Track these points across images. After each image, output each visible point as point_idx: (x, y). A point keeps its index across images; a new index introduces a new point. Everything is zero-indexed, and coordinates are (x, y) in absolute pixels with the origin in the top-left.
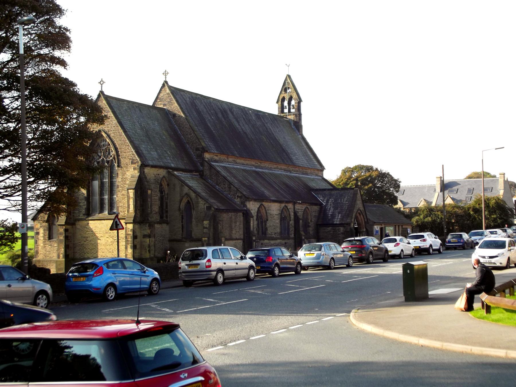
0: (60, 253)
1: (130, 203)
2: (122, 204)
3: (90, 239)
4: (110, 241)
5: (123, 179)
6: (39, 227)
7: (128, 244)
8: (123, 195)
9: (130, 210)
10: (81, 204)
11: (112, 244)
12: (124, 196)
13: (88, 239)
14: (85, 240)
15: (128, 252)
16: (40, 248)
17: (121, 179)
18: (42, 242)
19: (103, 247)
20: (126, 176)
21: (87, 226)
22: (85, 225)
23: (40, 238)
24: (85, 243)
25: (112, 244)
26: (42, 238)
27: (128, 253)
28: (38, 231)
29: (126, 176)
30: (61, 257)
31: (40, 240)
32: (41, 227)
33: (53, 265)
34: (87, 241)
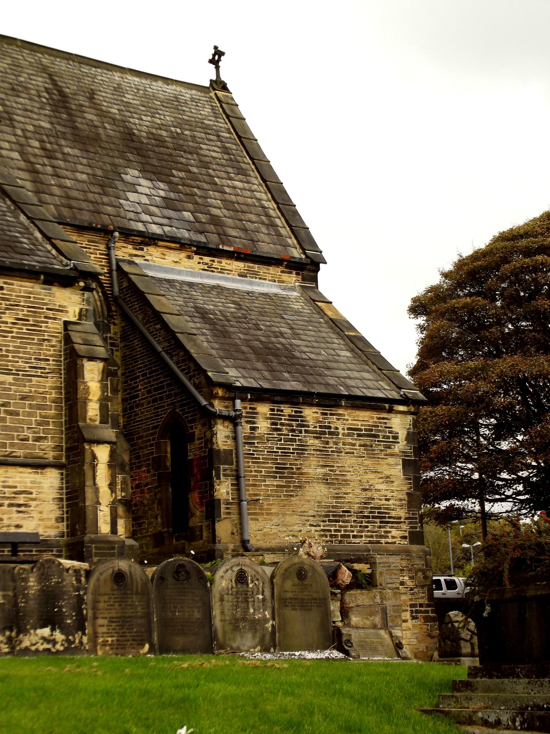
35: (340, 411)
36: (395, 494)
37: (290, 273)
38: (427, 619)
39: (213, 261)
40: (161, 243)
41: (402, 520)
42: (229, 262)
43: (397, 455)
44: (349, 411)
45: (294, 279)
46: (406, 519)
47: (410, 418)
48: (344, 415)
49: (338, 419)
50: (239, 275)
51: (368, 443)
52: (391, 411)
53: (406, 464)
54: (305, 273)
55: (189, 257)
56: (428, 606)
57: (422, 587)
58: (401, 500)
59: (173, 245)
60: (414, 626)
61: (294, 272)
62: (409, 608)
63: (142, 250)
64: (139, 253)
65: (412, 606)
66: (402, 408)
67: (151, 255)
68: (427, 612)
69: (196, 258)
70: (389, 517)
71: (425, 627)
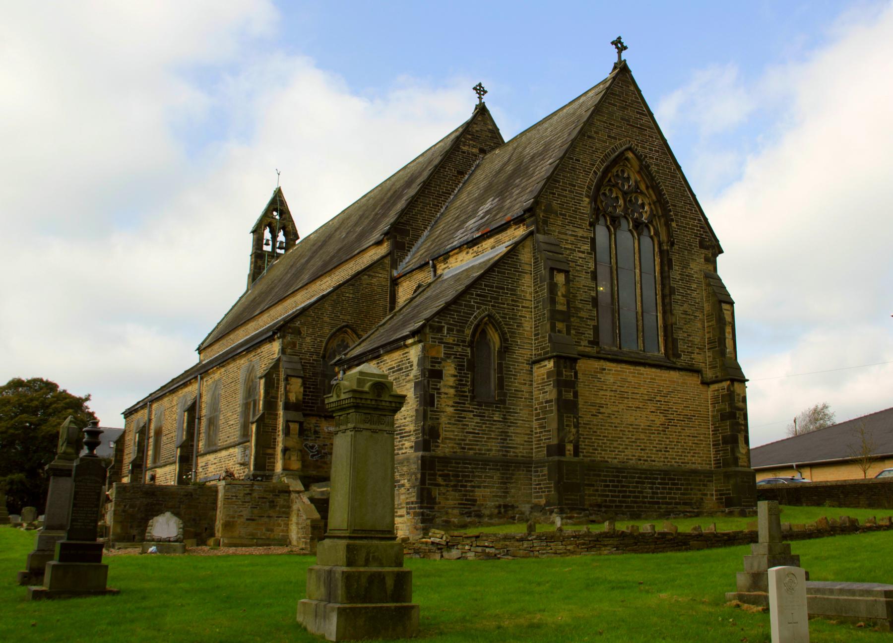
0: (566, 440)
1: (727, 334)
2: (685, 335)
3: (609, 411)
4: (658, 422)
5: (683, 275)
6: (442, 355)
7: (740, 433)
8: (685, 313)
9: (728, 350)
10: (583, 314)
11: (663, 431)
12: (689, 317)
13: (602, 410)
14: (594, 412)
15: (740, 452)
16: (444, 419)
17: (680, 274)
18: (451, 403)
19: (642, 436)
20: (689, 271)
21: (599, 375)
22: (595, 372)
23: (443, 390)
24: (595, 421)
25: (665, 431)
26: (452, 391)
27: (739, 455)
28: (437, 367)
29: (689, 271)
30: (567, 452)
31: (442, 396)
32: (448, 356)
33: (492, 478)
34: (600, 416)
35: (385, 358)
36: (409, 413)
37: (519, 227)
38: (416, 514)
39: (478, 247)
40: (451, 254)
41: (412, 433)
42: (486, 242)
43: (412, 380)
44: (389, 356)
45: (522, 230)
46: (414, 431)
47: (420, 346)
48: (386, 360)
49: (384, 364)
50: (491, 249)
51: (397, 377)
52: (406, 346)
53: (416, 384)
54: (528, 221)
55: (468, 253)
56: (416, 503)
57: (414, 487)
58: (412, 416)
59: (456, 251)
60: (408, 520)
61: (522, 225)
62: (405, 505)
63: (447, 262)
64: (446, 266)
65: (408, 503)
66: (410, 341)
67: (451, 263)
68: (414, 508)
69: (471, 251)
70: (405, 432)
71: (413, 520)
